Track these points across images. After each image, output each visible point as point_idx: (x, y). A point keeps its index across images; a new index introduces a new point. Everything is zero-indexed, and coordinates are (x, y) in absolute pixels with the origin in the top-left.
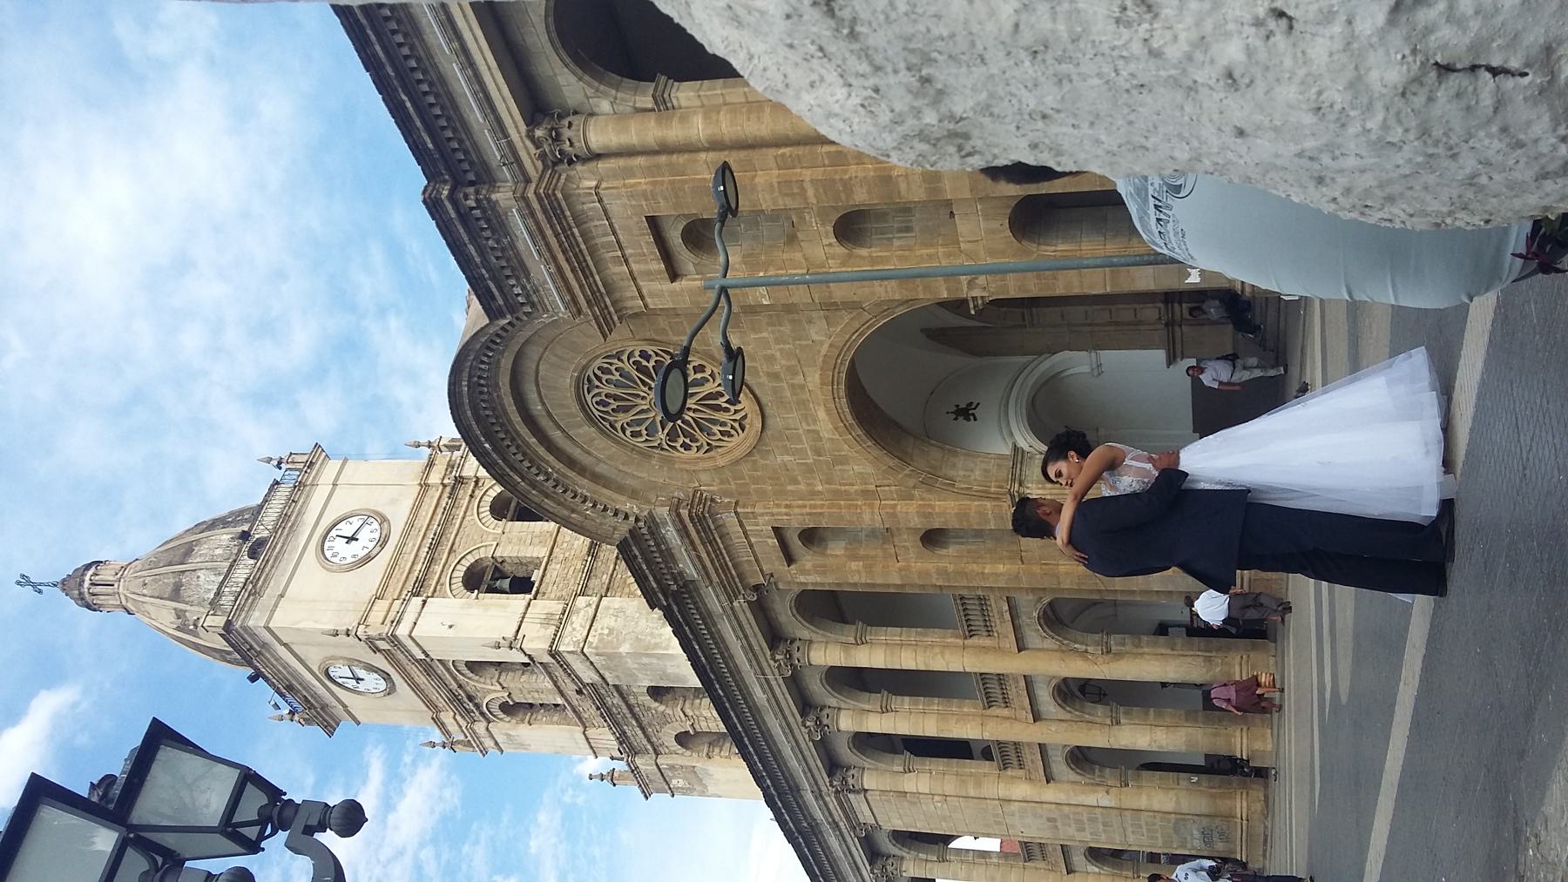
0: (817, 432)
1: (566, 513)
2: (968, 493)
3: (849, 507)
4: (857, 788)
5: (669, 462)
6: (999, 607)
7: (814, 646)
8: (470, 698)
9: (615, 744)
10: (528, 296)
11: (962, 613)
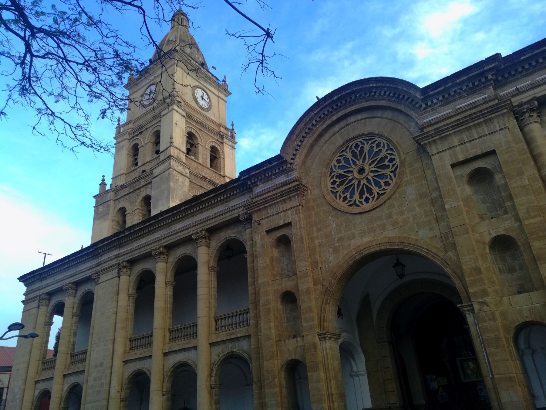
0: (354, 237)
4: (121, 273)
7: (207, 248)
8: (141, 133)
10: (430, 106)
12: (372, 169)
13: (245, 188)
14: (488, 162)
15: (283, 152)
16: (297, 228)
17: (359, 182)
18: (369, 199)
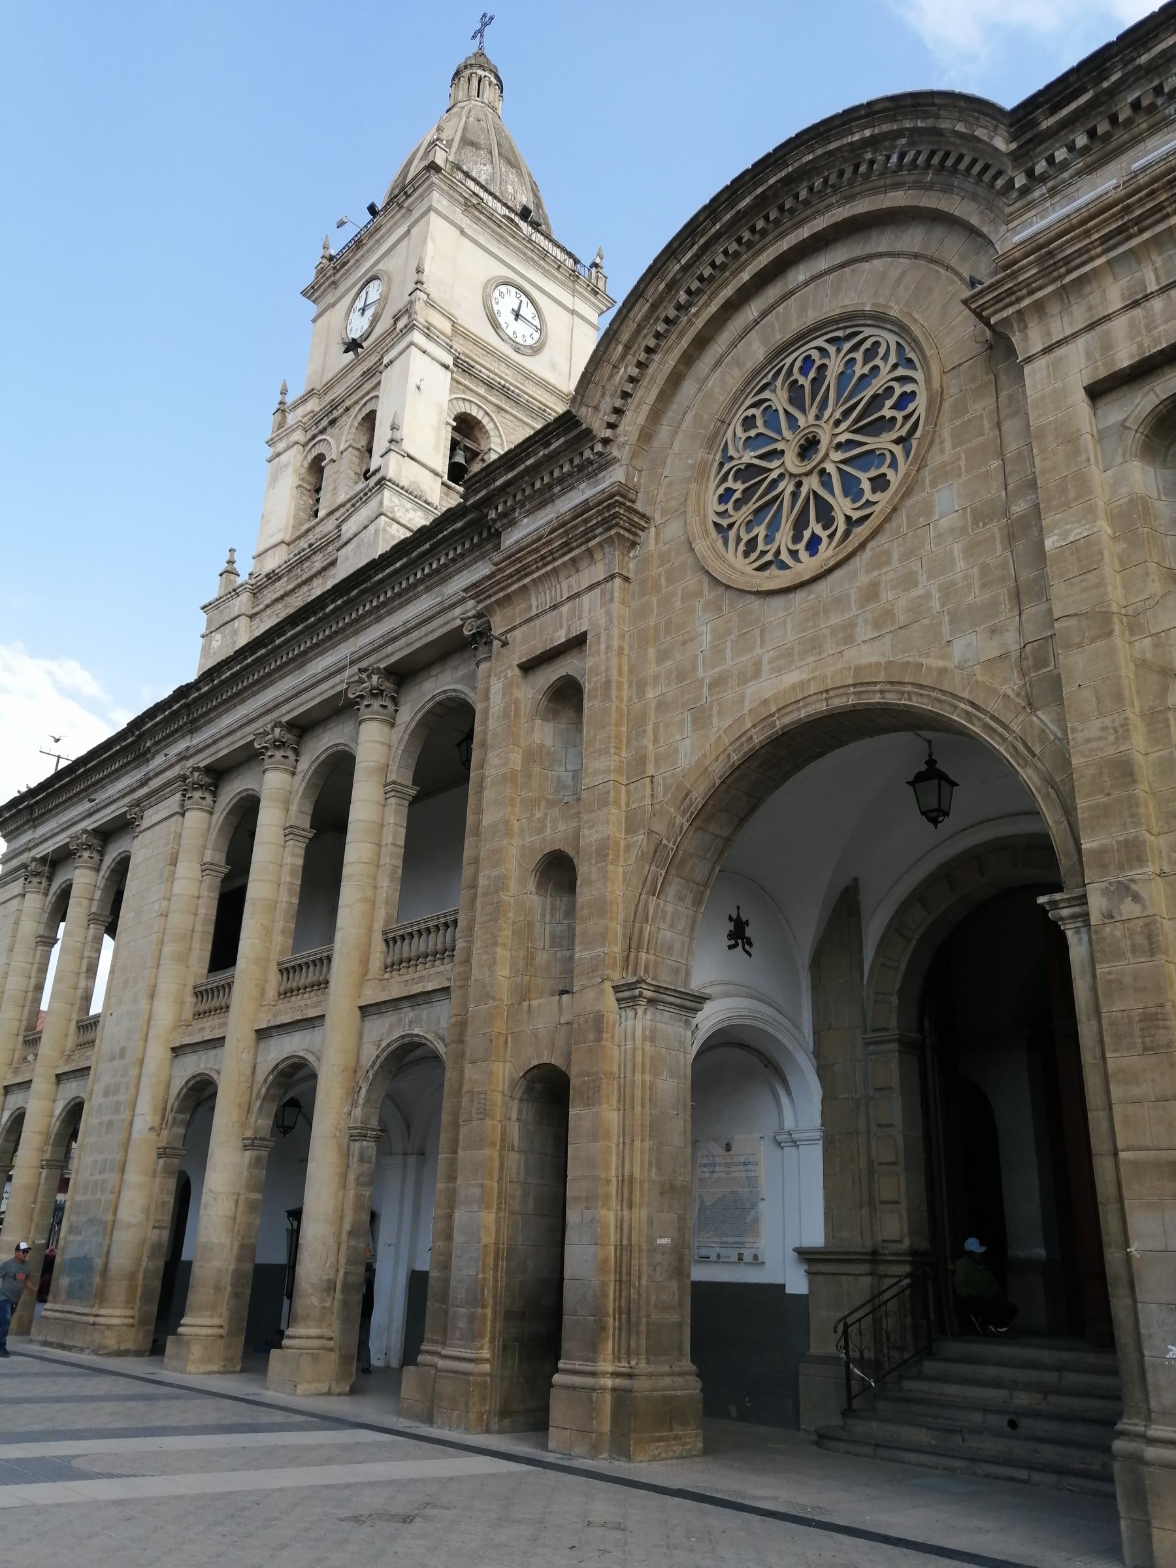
0: (757, 674)
1: (625, 337)
2: (638, 915)
3: (618, 737)
4: (187, 802)
5: (701, 472)
6: (431, 978)
8: (333, 422)
9: (265, 571)
10: (1043, 179)
11: (423, 926)
13: (485, 535)
15: (581, 402)
16: (599, 651)
17: (799, 485)
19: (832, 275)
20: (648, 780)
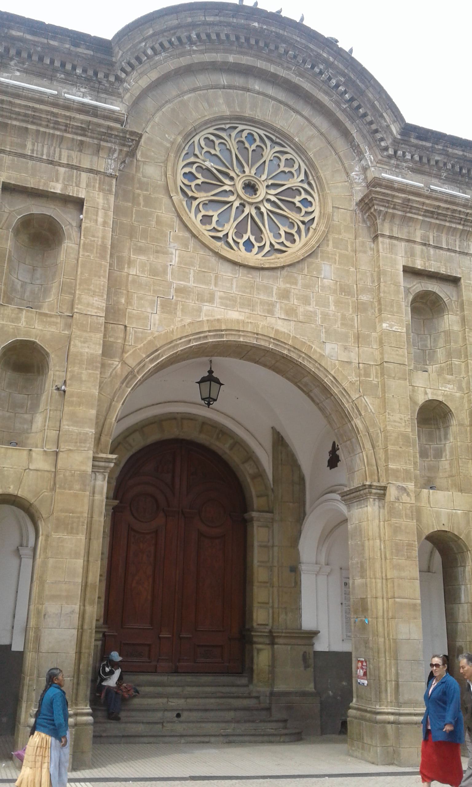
0: (211, 300)
12: (269, 197)
14: (445, 291)
17: (243, 205)
18: (253, 246)
19: (273, 102)
20: (123, 327)
